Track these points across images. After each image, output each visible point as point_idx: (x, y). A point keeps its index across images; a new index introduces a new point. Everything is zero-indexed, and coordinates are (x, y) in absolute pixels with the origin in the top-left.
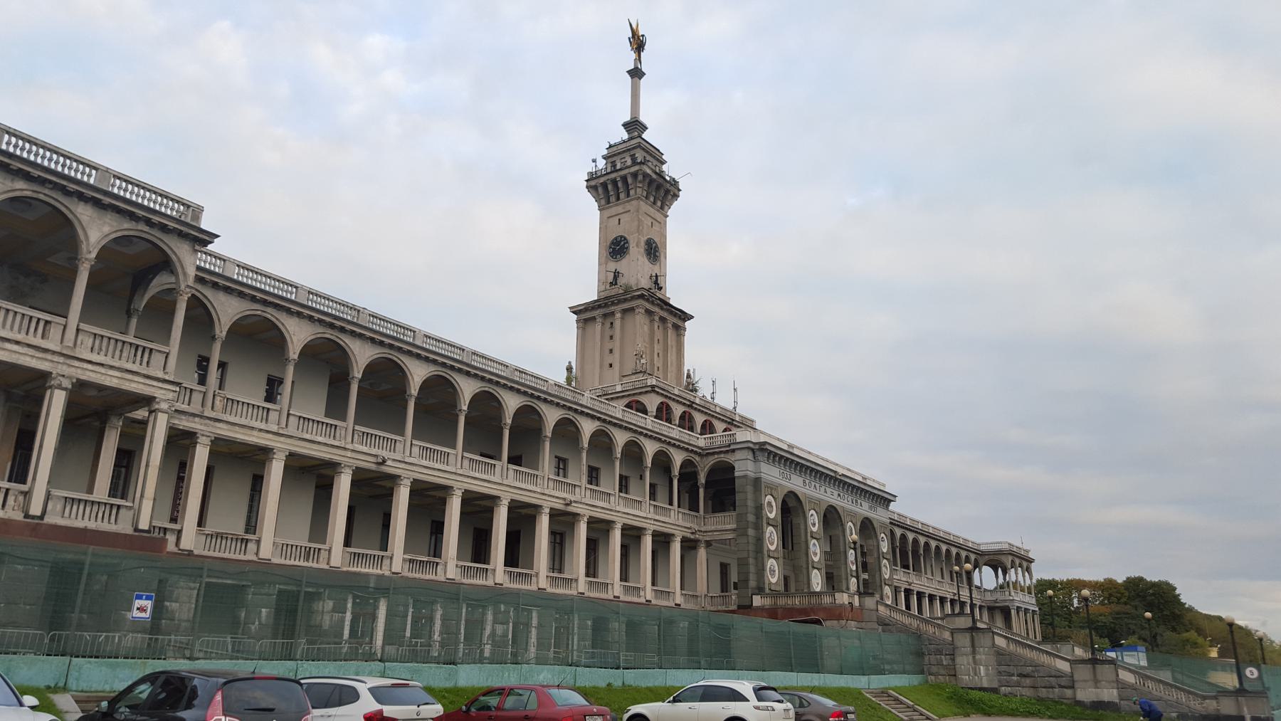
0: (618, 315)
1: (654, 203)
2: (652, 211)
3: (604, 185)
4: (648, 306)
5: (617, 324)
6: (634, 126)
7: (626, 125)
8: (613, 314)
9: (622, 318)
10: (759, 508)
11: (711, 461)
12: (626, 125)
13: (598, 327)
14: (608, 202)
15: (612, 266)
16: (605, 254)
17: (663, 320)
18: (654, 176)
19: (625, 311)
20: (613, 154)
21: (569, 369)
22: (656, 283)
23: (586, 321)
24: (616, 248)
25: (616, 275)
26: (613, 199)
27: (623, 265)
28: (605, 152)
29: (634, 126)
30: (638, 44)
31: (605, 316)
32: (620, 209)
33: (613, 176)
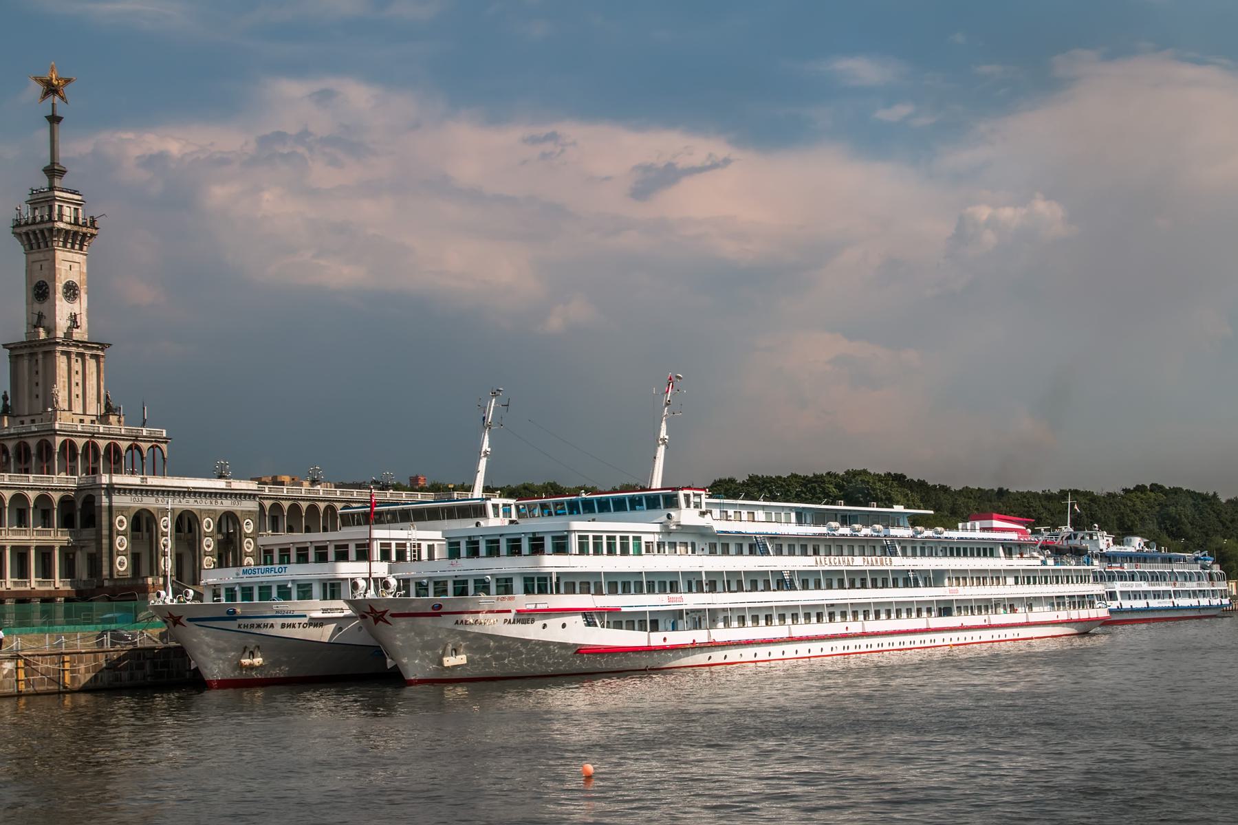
0: (40, 356)
1: (73, 247)
2: (69, 256)
3: (27, 234)
4: (65, 349)
5: (40, 362)
6: (53, 171)
7: (46, 170)
8: (36, 354)
9: (44, 358)
10: (111, 525)
11: (84, 494)
12: (46, 170)
15: (38, 307)
16: (31, 295)
17: (82, 355)
18: (69, 227)
21: (5, 398)
22: (75, 321)
23: (17, 356)
25: (40, 316)
26: (35, 246)
28: (29, 198)
30: (51, 89)
31: (31, 354)
33: (33, 227)
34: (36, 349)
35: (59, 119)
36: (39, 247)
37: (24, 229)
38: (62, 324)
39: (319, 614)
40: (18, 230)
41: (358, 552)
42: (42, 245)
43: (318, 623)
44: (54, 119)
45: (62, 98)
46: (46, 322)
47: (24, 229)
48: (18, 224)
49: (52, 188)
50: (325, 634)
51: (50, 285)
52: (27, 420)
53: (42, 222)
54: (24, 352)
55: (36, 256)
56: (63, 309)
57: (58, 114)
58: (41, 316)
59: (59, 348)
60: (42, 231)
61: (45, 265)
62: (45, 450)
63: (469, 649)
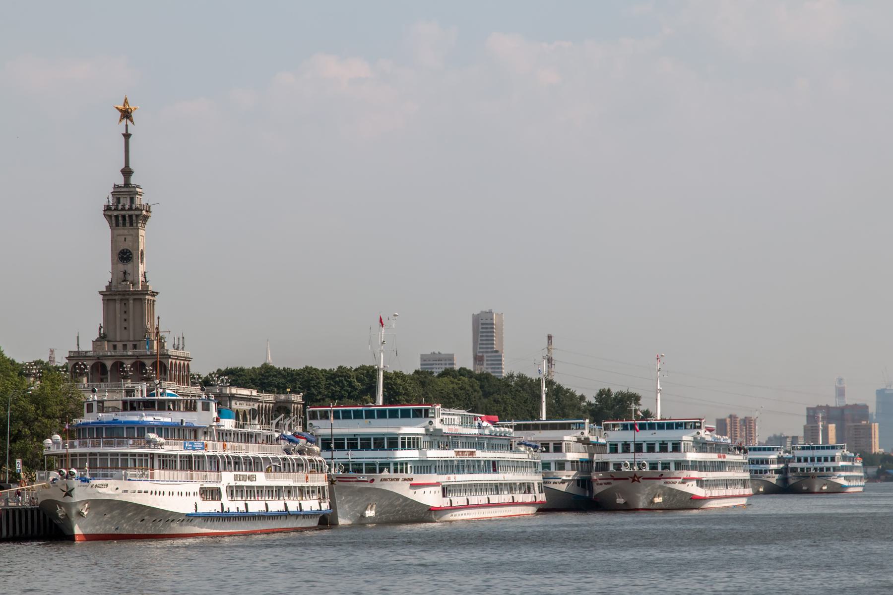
0: (131, 302)
3: (117, 217)
5: (131, 306)
6: (127, 172)
13: (118, 306)
14: (117, 225)
15: (121, 267)
16: (116, 258)
19: (134, 299)
20: (117, 193)
24: (125, 256)
25: (125, 273)
27: (129, 267)
29: (127, 172)
30: (126, 114)
32: (126, 232)
33: (123, 213)
34: (127, 297)
35: (129, 135)
36: (124, 225)
37: (116, 213)
38: (141, 279)
39: (564, 478)
40: (109, 213)
41: (554, 448)
42: (128, 225)
43: (563, 482)
44: (127, 136)
45: (132, 121)
46: (130, 278)
47: (116, 213)
48: (108, 208)
49: (127, 184)
50: (563, 488)
51: (134, 253)
52: (120, 346)
53: (123, 209)
54: (117, 297)
55: (121, 231)
56: (142, 268)
57: (129, 132)
58: (125, 273)
59: (147, 297)
60: (131, 216)
61: (129, 238)
62: (139, 366)
63: (664, 495)
